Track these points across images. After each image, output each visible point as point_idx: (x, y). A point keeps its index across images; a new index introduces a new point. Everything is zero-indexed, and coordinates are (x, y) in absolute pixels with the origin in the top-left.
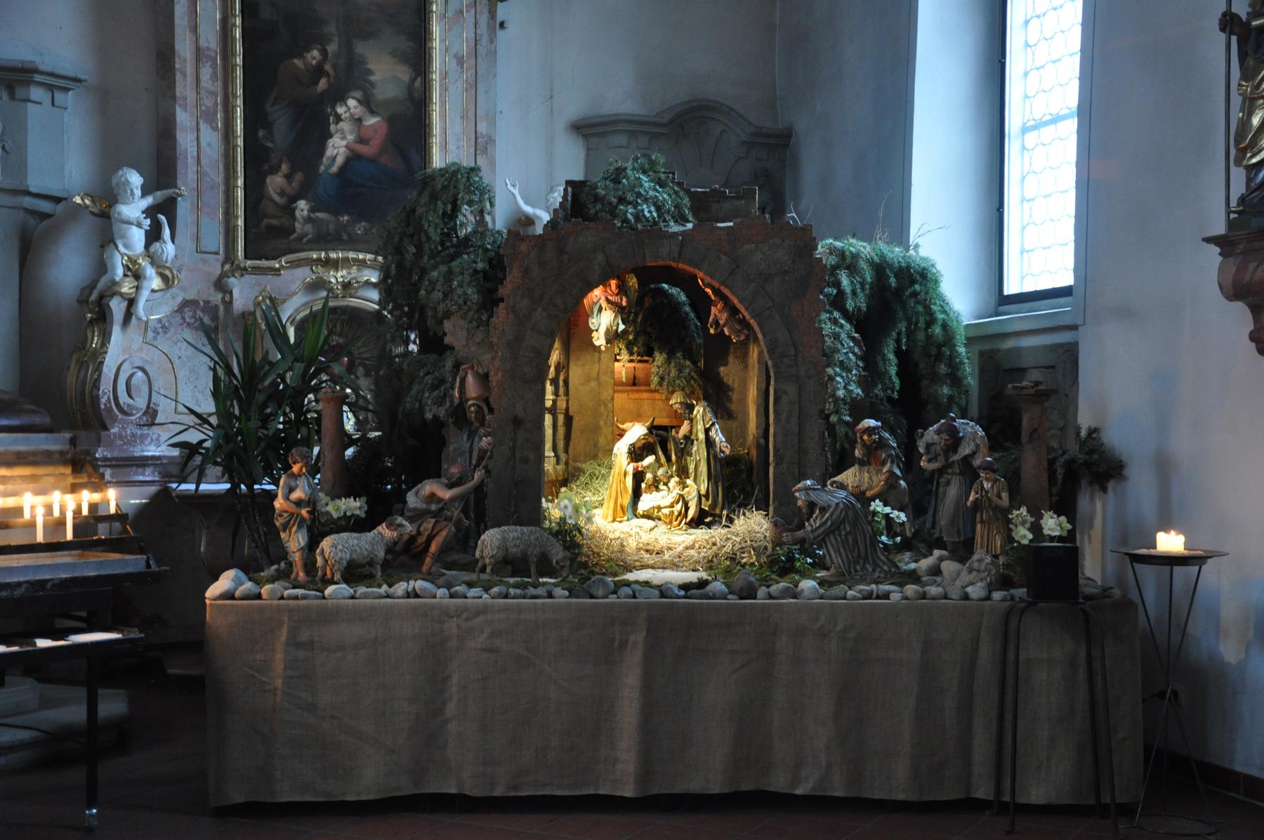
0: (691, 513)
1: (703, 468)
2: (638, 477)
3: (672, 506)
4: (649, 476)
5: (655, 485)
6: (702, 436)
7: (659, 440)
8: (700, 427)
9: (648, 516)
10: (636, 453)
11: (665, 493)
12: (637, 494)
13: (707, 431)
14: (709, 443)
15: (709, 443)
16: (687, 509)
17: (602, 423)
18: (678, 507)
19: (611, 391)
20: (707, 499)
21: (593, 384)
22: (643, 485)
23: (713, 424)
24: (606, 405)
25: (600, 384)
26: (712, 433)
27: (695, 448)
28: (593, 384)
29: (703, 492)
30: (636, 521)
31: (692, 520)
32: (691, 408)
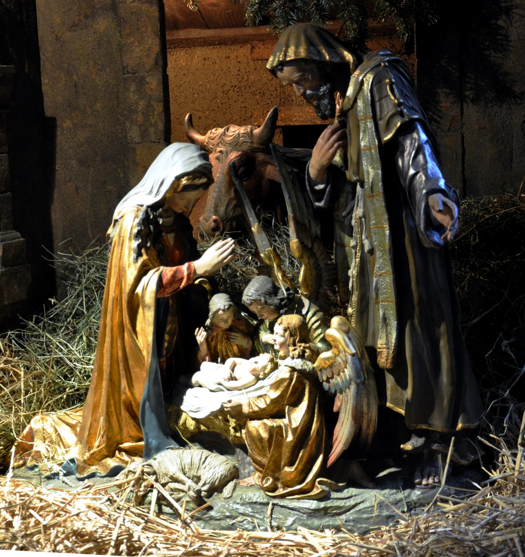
0: (343, 432)
1: (383, 278)
2: (181, 308)
3: (276, 411)
4: (219, 302)
5: (244, 336)
6: (372, 171)
7: (266, 187)
8: (366, 140)
9: (212, 437)
10: (168, 233)
11: (263, 359)
12: (176, 370)
13: (389, 153)
14: (397, 193)
15: (397, 193)
16: (330, 419)
17: (134, 133)
18: (298, 415)
19: (153, 42)
20: (402, 384)
21: (103, 24)
22: (201, 336)
23: (407, 129)
24: (141, 82)
25: (120, 22)
26: (405, 159)
27: (358, 212)
28: (103, 24)
29: (384, 359)
30: (170, 460)
31: (344, 455)
32: (339, 76)
